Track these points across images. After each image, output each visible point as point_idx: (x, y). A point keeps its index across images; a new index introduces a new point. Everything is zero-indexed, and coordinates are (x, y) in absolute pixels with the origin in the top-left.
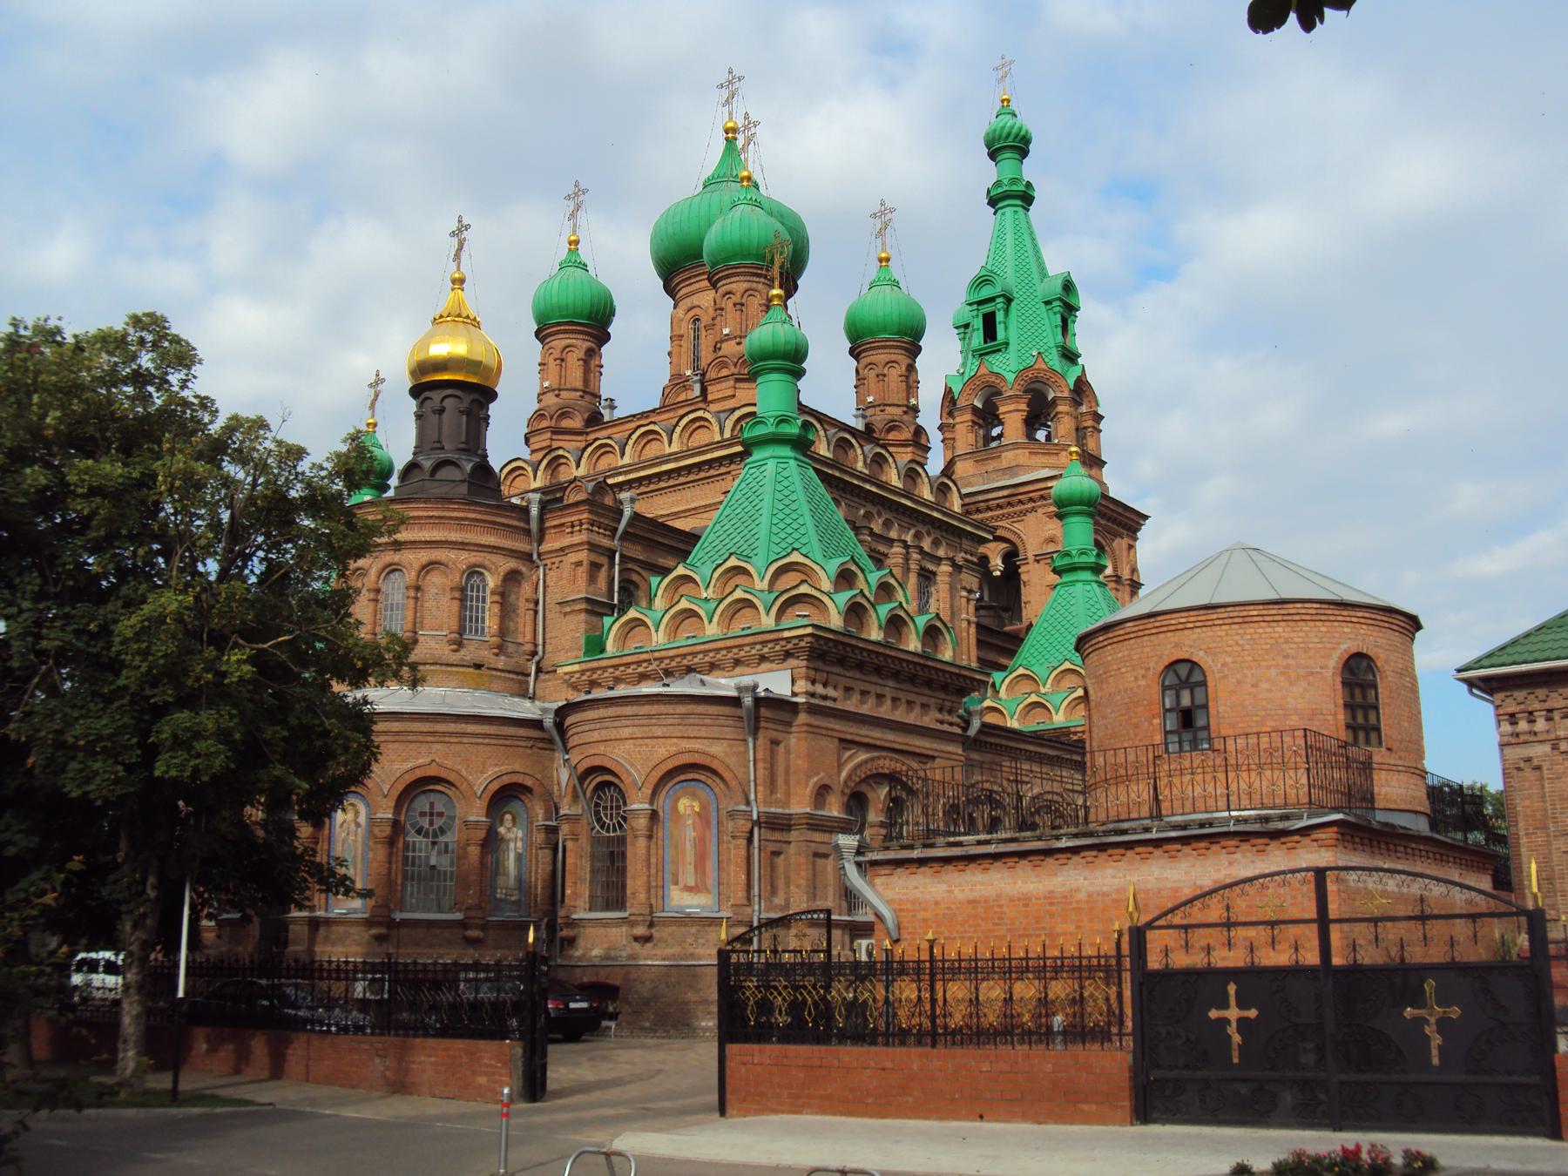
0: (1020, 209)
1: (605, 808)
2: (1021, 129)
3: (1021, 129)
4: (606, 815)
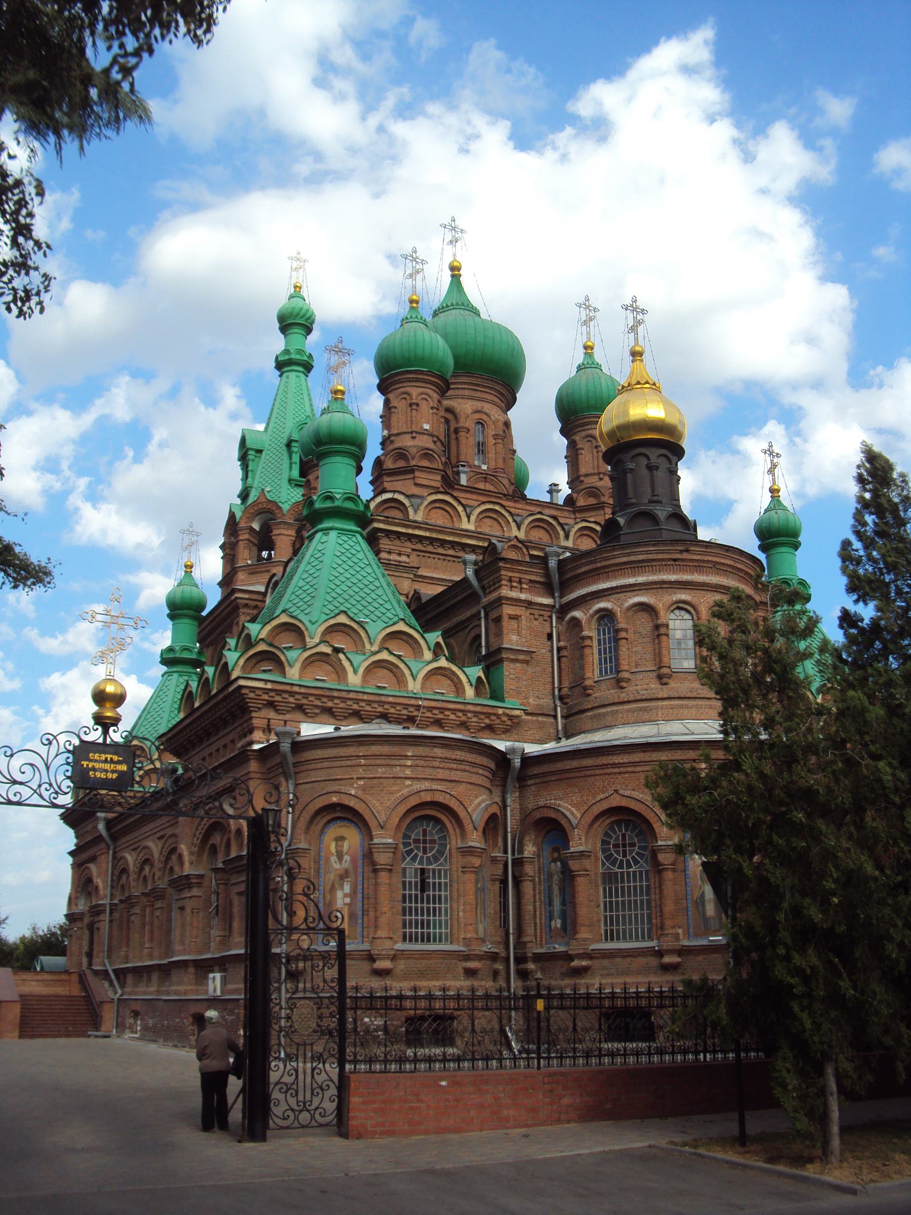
0: (302, 375)
1: (616, 846)
2: (308, 311)
3: (308, 311)
4: (618, 853)
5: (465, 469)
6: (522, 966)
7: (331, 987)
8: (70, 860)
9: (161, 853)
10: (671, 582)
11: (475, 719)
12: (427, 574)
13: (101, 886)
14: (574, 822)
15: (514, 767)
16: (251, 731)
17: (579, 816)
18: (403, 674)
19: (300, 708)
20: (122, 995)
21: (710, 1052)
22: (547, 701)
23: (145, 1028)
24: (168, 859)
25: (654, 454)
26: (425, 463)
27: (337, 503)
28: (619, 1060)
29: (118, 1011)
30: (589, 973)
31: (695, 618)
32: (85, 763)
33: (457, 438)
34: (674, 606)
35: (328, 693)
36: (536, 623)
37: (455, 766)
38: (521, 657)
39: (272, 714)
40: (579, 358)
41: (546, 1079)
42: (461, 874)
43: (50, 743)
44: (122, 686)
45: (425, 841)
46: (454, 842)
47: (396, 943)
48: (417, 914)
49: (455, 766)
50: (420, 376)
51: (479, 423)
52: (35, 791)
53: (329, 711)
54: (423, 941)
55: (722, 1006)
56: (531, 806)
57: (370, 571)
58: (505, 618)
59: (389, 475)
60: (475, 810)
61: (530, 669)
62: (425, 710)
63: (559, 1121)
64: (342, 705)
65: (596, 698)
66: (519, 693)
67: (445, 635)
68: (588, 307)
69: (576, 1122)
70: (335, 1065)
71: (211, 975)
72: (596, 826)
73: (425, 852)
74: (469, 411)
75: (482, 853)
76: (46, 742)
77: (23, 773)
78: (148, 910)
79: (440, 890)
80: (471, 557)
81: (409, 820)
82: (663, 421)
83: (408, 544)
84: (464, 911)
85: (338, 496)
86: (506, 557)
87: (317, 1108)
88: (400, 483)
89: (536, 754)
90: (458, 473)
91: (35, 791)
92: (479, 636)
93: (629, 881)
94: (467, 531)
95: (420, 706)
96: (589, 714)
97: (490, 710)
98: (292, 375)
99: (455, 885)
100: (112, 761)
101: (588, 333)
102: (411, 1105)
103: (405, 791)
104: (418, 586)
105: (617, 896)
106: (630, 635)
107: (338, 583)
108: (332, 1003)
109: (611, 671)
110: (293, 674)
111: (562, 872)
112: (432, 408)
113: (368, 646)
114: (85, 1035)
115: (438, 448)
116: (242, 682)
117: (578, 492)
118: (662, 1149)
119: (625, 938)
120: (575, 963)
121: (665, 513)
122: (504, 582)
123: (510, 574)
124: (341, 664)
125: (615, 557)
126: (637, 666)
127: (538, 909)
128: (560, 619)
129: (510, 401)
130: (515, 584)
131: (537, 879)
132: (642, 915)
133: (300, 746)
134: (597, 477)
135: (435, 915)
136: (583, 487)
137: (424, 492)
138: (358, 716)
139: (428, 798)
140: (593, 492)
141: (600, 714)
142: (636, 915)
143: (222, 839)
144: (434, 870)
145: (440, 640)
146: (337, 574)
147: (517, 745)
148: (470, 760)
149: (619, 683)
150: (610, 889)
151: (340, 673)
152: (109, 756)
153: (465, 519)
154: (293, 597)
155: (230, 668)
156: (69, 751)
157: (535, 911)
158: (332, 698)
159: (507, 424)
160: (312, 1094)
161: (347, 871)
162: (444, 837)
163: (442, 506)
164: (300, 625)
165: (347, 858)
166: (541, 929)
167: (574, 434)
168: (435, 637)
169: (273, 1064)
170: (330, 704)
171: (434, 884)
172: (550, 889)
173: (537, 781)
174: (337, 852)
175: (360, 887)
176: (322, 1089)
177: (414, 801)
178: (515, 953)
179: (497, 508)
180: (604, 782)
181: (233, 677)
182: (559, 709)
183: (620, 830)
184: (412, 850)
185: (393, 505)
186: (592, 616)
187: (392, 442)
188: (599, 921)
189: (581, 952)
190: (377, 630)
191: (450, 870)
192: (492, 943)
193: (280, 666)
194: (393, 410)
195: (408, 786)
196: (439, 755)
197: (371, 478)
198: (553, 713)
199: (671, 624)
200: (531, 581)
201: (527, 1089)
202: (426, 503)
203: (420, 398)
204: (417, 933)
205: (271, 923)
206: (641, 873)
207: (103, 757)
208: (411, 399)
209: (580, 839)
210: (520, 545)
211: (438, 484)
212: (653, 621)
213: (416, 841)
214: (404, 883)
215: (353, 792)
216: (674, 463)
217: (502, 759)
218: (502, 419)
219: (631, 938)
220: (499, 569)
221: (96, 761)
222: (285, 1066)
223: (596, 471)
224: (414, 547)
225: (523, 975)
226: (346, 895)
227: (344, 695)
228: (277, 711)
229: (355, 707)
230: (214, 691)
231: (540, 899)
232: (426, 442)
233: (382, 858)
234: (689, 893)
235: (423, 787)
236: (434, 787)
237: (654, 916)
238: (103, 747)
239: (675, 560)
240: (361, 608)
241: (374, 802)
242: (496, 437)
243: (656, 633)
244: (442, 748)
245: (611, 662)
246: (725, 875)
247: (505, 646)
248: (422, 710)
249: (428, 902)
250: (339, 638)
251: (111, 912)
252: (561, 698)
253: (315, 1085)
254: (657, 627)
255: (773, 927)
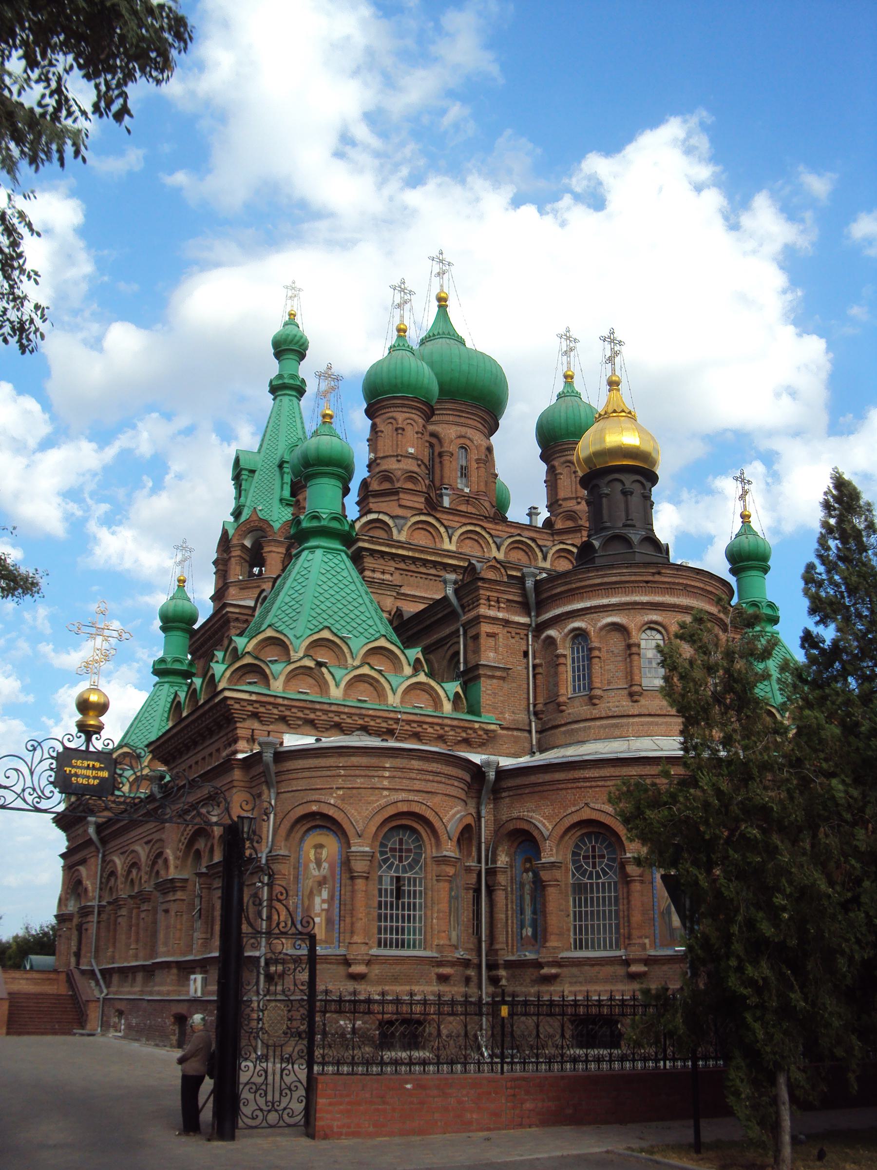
0: (295, 399)
1: (586, 857)
2: (302, 337)
3: (302, 337)
4: (588, 864)
5: (448, 492)
6: (494, 973)
7: (302, 991)
8: (61, 862)
9: (148, 856)
10: (642, 604)
11: (452, 733)
12: (409, 593)
13: (90, 887)
14: (546, 833)
15: (489, 780)
16: (236, 741)
17: (550, 827)
18: (384, 689)
19: (283, 719)
20: (107, 995)
21: (669, 1060)
22: (522, 717)
23: (129, 1027)
24: (154, 863)
25: (628, 479)
26: (409, 486)
27: (323, 523)
28: (581, 1066)
29: (103, 1011)
30: (558, 980)
31: (666, 638)
32: (68, 769)
33: (441, 462)
34: (646, 627)
35: (310, 706)
36: (513, 641)
37: (431, 778)
38: (498, 674)
39: (256, 725)
40: (560, 387)
41: (509, 1084)
42: (435, 882)
43: (35, 749)
44: (105, 695)
45: (401, 850)
46: (429, 851)
47: (371, 948)
48: (392, 921)
49: (431, 778)
50: (406, 402)
51: (462, 447)
52: (19, 796)
53: (311, 723)
54: (397, 946)
55: (679, 1015)
56: (504, 818)
57: (354, 588)
58: (483, 636)
59: (374, 496)
60: (450, 820)
61: (506, 686)
62: (403, 724)
63: (521, 1125)
64: (324, 717)
65: (569, 714)
66: (495, 708)
67: (425, 652)
68: (568, 338)
69: (537, 1126)
70: (304, 1066)
71: (193, 977)
72: (567, 838)
73: (401, 861)
74: (453, 436)
75: (456, 862)
76: (31, 748)
77: (8, 777)
78: (135, 911)
79: (415, 898)
80: (452, 577)
81: (386, 829)
82: (638, 448)
83: (392, 563)
84: (438, 918)
85: (324, 516)
86: (485, 577)
87: (285, 1109)
88: (385, 504)
89: (510, 767)
90: (441, 496)
91: (19, 796)
92: (458, 653)
93: (598, 892)
94: (448, 551)
95: (399, 719)
96: (563, 729)
97: (467, 725)
98: (286, 399)
99: (430, 893)
100: (94, 768)
101: (569, 363)
102: (377, 1106)
103: (383, 802)
104: (399, 604)
105: (586, 906)
106: (603, 654)
107: (323, 599)
108: (302, 1006)
109: (584, 688)
110: (277, 686)
111: (534, 882)
112: (417, 433)
113: (350, 661)
114: (69, 1033)
115: (422, 471)
116: (227, 694)
117: (557, 516)
118: (620, 1155)
119: (593, 947)
120: (545, 971)
121: (639, 537)
122: (482, 601)
123: (488, 593)
124: (324, 678)
125: (589, 578)
126: (609, 683)
127: (510, 917)
128: (536, 637)
129: (493, 427)
130: (492, 603)
131: (509, 889)
132: (610, 925)
133: (282, 756)
134: (574, 502)
135: (409, 922)
136: (561, 510)
137: (407, 513)
138: (339, 728)
139: (404, 808)
140: (571, 516)
141: (572, 729)
142: (604, 925)
143: (206, 845)
144: (409, 879)
145: (420, 656)
146: (322, 591)
147: (492, 758)
148: (446, 772)
149: (591, 700)
150: (580, 899)
151: (323, 686)
152: (91, 763)
153: (446, 540)
154: (279, 612)
155: (217, 680)
156: (52, 758)
157: (507, 920)
158: (314, 710)
159: (490, 449)
160: (281, 1094)
161: (325, 877)
162: (420, 847)
163: (424, 526)
164: (285, 640)
165: (325, 865)
166: (512, 937)
167: (553, 460)
168: (415, 653)
169: (243, 1064)
170: (312, 716)
171: (409, 891)
172: (522, 898)
173: (511, 793)
174: (316, 859)
175: (337, 893)
176: (290, 1090)
177: (391, 811)
178: (487, 960)
179: (478, 529)
180: (575, 795)
181: (220, 688)
182: (533, 724)
183: (591, 842)
184: (387, 859)
185: (378, 525)
186: (567, 635)
187: (378, 464)
188: (569, 930)
189: (551, 959)
190: (359, 645)
191: (425, 878)
192: (465, 949)
193: (265, 679)
194: (380, 434)
195: (386, 796)
196: (416, 767)
197: (357, 499)
198: (527, 728)
199: (643, 644)
200: (508, 600)
201: (490, 1093)
202: (410, 524)
203: (405, 423)
204: (391, 939)
205: (245, 928)
206: (610, 883)
207: (86, 763)
208: (398, 424)
209: (551, 850)
210: (498, 566)
211: (422, 506)
212: (625, 640)
213: (393, 850)
214: (380, 890)
215: (332, 802)
216: (648, 488)
217: (477, 772)
218: (484, 444)
219: (599, 947)
220: (478, 588)
221: (79, 767)
222: (255, 1067)
223: (574, 495)
224: (397, 566)
225: (494, 981)
226: (323, 901)
227: (326, 707)
228: (261, 721)
229: (337, 719)
230: (201, 702)
231: (512, 908)
232: (411, 465)
233: (359, 866)
234: (656, 904)
235: (400, 798)
236: (411, 798)
237: (621, 926)
238: (86, 754)
239: (647, 582)
240: (344, 624)
241: (352, 811)
242: (478, 461)
243: (628, 652)
244: (419, 760)
245: (584, 680)
246: (683, 888)
247: (482, 663)
248: (401, 723)
249: (403, 909)
250: (322, 652)
251: (99, 914)
252: (536, 714)
253: (284, 1086)
254: (629, 646)
255: (727, 939)
